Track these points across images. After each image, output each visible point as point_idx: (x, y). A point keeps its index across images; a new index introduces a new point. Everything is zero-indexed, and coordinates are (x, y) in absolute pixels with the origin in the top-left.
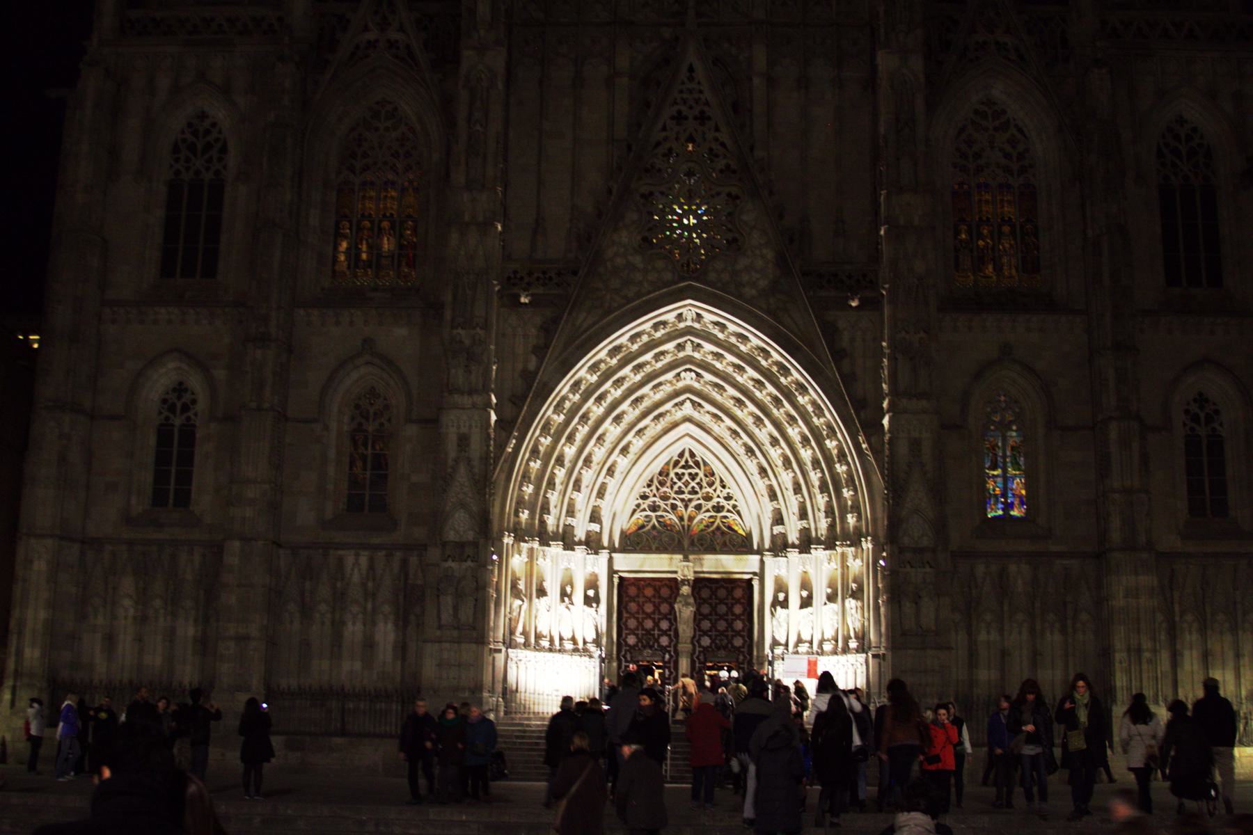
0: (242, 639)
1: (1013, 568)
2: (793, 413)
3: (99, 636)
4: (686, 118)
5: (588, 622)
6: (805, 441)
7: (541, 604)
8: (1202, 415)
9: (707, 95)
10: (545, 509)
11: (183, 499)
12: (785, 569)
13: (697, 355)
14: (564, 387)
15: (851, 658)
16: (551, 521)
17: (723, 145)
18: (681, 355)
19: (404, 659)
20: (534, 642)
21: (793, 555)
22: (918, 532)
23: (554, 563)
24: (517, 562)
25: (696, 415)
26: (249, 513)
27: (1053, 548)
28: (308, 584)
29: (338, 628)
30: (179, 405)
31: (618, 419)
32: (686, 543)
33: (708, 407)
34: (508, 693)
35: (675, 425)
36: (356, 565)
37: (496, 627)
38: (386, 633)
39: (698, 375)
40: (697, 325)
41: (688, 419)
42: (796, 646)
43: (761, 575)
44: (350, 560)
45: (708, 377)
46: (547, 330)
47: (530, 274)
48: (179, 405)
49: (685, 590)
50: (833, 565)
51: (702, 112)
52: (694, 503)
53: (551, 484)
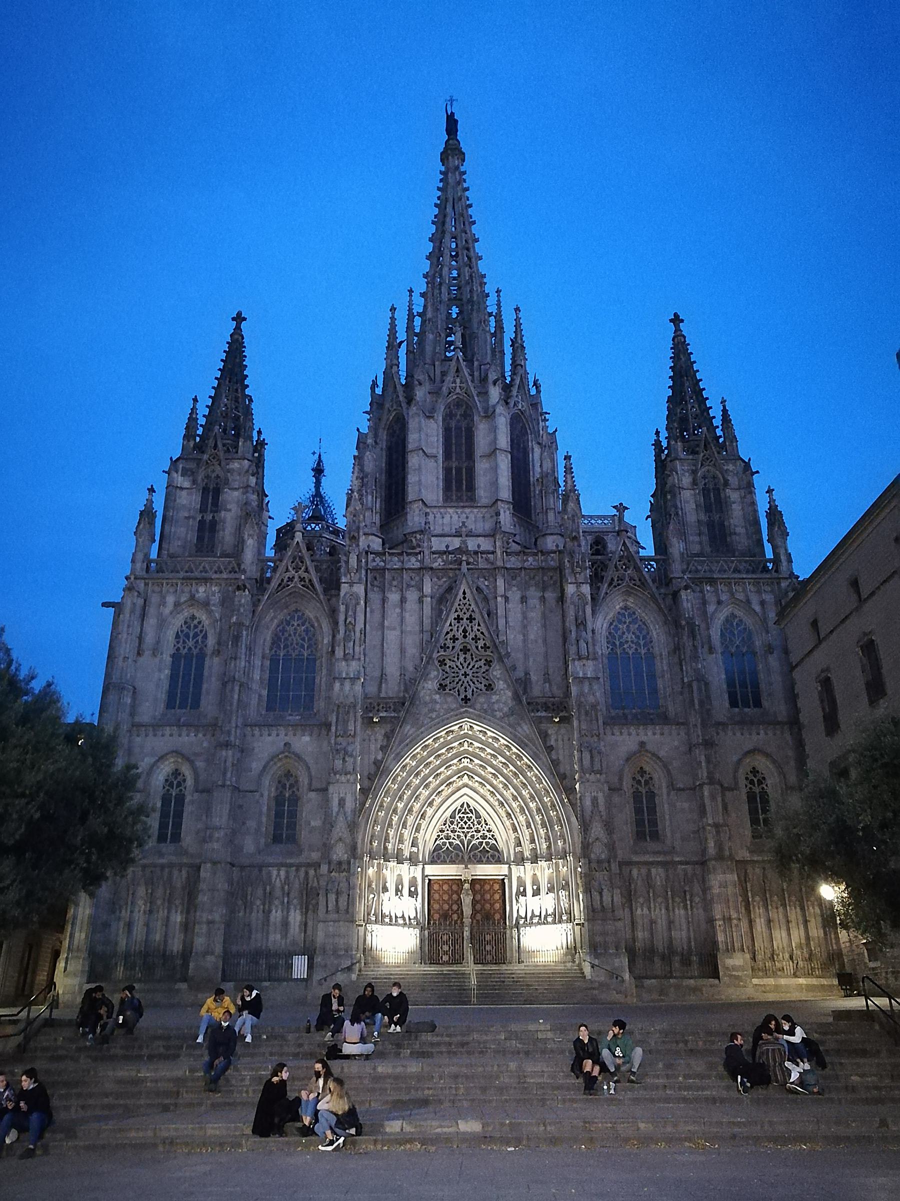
0: (210, 922)
1: (653, 871)
2: (524, 781)
3: (122, 924)
4: (462, 619)
5: (411, 907)
6: (532, 798)
7: (385, 897)
8: (756, 780)
9: (473, 606)
10: (387, 840)
11: (176, 838)
12: (525, 873)
13: (470, 749)
14: (397, 769)
15: (564, 925)
16: (390, 846)
17: (482, 633)
18: (462, 749)
19: (305, 932)
20: (381, 919)
21: (528, 865)
22: (599, 851)
23: (393, 872)
24: (371, 872)
25: (470, 783)
26: (216, 846)
28: (250, 889)
29: (267, 913)
30: (175, 783)
31: (427, 786)
32: (466, 857)
33: (477, 778)
34: (367, 951)
35: (459, 789)
36: (277, 876)
37: (360, 910)
38: (295, 917)
39: (471, 760)
40: (470, 733)
41: (466, 786)
42: (531, 918)
43: (509, 876)
44: (275, 873)
45: (477, 761)
46: (388, 736)
47: (379, 705)
48: (175, 783)
49: (467, 886)
50: (551, 870)
51: (471, 616)
52: (470, 834)
53: (390, 825)
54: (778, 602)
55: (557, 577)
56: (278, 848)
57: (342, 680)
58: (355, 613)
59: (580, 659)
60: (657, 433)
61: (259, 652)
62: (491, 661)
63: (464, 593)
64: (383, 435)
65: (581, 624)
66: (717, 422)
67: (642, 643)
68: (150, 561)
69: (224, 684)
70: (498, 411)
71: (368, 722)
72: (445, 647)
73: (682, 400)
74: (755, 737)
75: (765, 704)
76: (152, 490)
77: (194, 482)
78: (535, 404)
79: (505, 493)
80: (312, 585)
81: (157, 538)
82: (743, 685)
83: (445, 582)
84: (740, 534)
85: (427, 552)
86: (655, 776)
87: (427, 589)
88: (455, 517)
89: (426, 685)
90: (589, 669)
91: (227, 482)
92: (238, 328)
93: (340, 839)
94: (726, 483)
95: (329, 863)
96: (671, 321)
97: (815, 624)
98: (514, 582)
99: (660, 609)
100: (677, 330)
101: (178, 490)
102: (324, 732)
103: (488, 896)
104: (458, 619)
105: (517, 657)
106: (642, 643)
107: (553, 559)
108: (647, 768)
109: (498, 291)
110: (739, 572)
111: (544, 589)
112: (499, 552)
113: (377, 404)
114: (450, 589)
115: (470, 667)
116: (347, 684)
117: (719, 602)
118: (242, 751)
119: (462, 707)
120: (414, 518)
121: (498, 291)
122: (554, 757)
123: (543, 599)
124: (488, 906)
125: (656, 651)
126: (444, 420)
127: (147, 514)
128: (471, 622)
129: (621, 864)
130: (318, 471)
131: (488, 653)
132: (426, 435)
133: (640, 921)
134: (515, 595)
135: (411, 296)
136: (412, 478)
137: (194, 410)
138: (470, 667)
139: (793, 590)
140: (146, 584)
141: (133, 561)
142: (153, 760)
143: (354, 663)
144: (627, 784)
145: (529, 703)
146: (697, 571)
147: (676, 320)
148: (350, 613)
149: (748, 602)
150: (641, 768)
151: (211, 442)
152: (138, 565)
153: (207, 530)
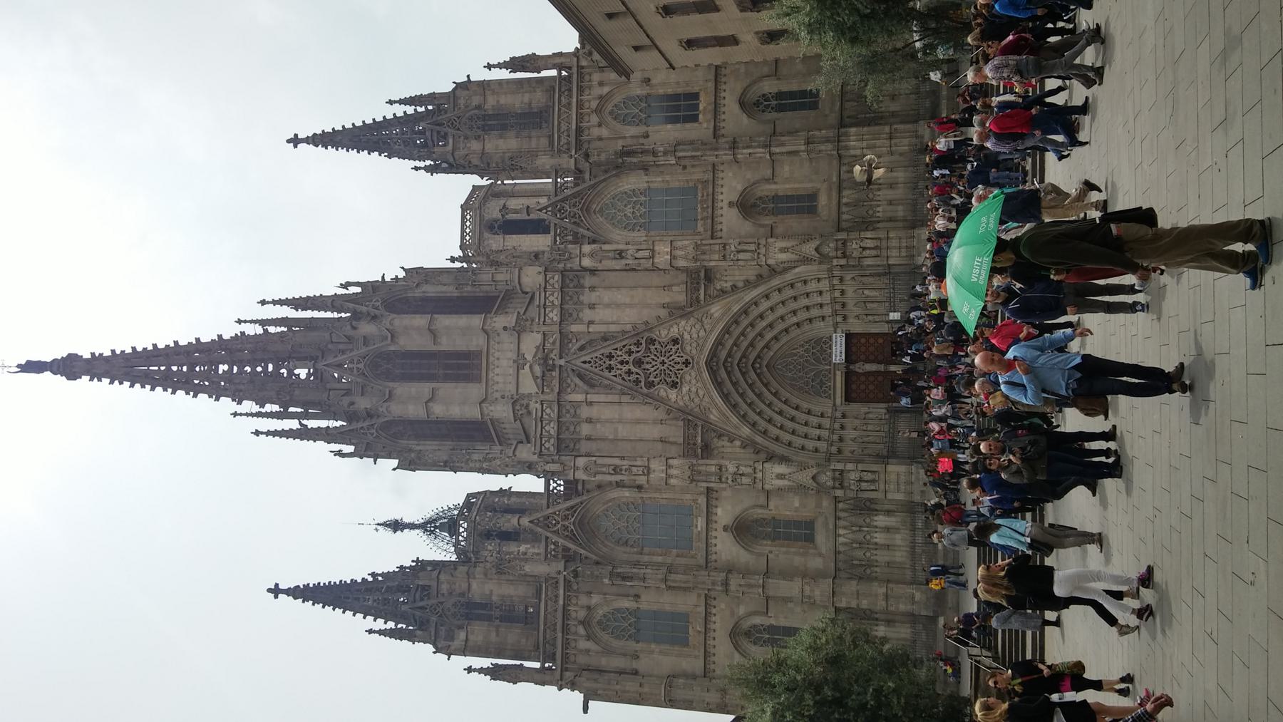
0: (887, 597)
1: (845, 200)
9: (597, 354)
26: (817, 592)
27: (835, 179)
36: (845, 536)
38: (881, 520)
44: (841, 540)
46: (720, 436)
54: (601, 69)
55: (571, 275)
56: (821, 538)
57: (668, 476)
58: (604, 465)
59: (653, 257)
60: (416, 168)
61: (636, 557)
64: (404, 442)
65: (620, 255)
66: (410, 110)
68: (543, 665)
69: (669, 588)
70: (388, 326)
71: (707, 450)
72: (637, 382)
73: (384, 143)
74: (726, 102)
75: (696, 89)
76: (469, 670)
77: (460, 627)
78: (371, 288)
79: (476, 320)
80: (572, 507)
81: (518, 662)
82: (677, 108)
85: (542, 397)
86: (759, 194)
87: (579, 397)
88: (497, 370)
90: (663, 249)
91: (462, 595)
92: (288, 592)
93: (814, 478)
94: (478, 107)
96: (295, 146)
97: (636, 48)
98: (575, 315)
99: (604, 180)
100: (307, 140)
101: (470, 644)
102: (715, 494)
103: (863, 349)
104: (610, 368)
105: (647, 315)
109: (239, 322)
110: (570, 104)
111: (583, 287)
112: (545, 328)
113: (368, 449)
116: (673, 472)
117: (600, 125)
118: (730, 571)
120: (501, 411)
121: (239, 322)
122: (740, 284)
123: (592, 288)
124: (872, 349)
125: (643, 186)
126: (393, 380)
127: (495, 673)
129: (839, 230)
130: (396, 526)
132: (410, 400)
133: (889, 214)
134: (587, 314)
135: (241, 414)
136: (456, 412)
137: (380, 632)
139: (590, 54)
140: (567, 670)
141: (543, 684)
142: (737, 655)
143: (652, 466)
144: (768, 221)
146: (568, 143)
147: (295, 141)
149: (601, 97)
151: (418, 613)
152: (547, 678)
153: (508, 615)
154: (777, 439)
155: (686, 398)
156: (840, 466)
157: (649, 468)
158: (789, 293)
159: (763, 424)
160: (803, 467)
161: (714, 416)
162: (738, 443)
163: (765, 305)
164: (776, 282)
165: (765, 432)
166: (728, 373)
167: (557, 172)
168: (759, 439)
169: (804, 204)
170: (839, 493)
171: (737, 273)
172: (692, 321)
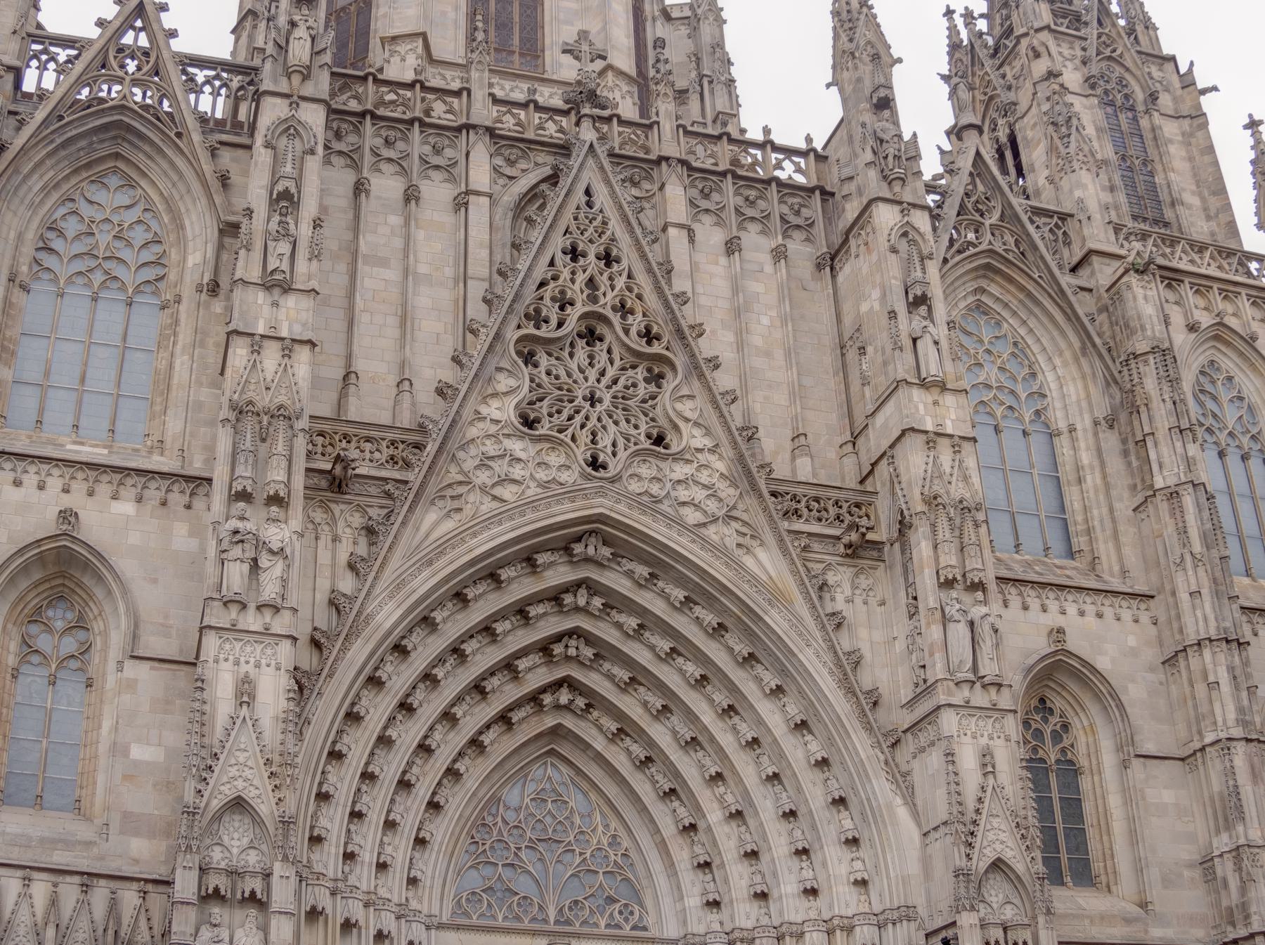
4: (584, 255)
9: (615, 226)
17: (640, 297)
46: (370, 531)
57: (257, 342)
59: (924, 384)
62: (661, 376)
63: (588, 192)
67: (1023, 396)
83: (523, 171)
84: (1189, 207)
89: (484, 410)
94: (1153, 97)
95: (203, 870)
98: (704, 204)
99: (1072, 316)
104: (574, 253)
106: (1023, 396)
107: (798, 170)
108: (1057, 703)
114: (553, 180)
115: (605, 381)
116: (271, 358)
119: (588, 478)
122: (845, 642)
128: (608, 265)
131: (656, 348)
134: (711, 236)
138: (605, 381)
143: (291, 301)
145: (774, 494)
148: (288, 169)
150: (1042, 701)
154: (353, 717)
155: (490, 448)
156: (282, 894)
157: (286, 288)
158: (815, 793)
159: (400, 677)
160: (278, 770)
161: (432, 523)
162: (347, 584)
163: (774, 717)
164: (861, 744)
165: (374, 682)
166: (555, 597)
167: (1064, 217)
168: (359, 653)
169: (1065, 848)
170: (186, 885)
171: (878, 636)
172: (728, 492)
